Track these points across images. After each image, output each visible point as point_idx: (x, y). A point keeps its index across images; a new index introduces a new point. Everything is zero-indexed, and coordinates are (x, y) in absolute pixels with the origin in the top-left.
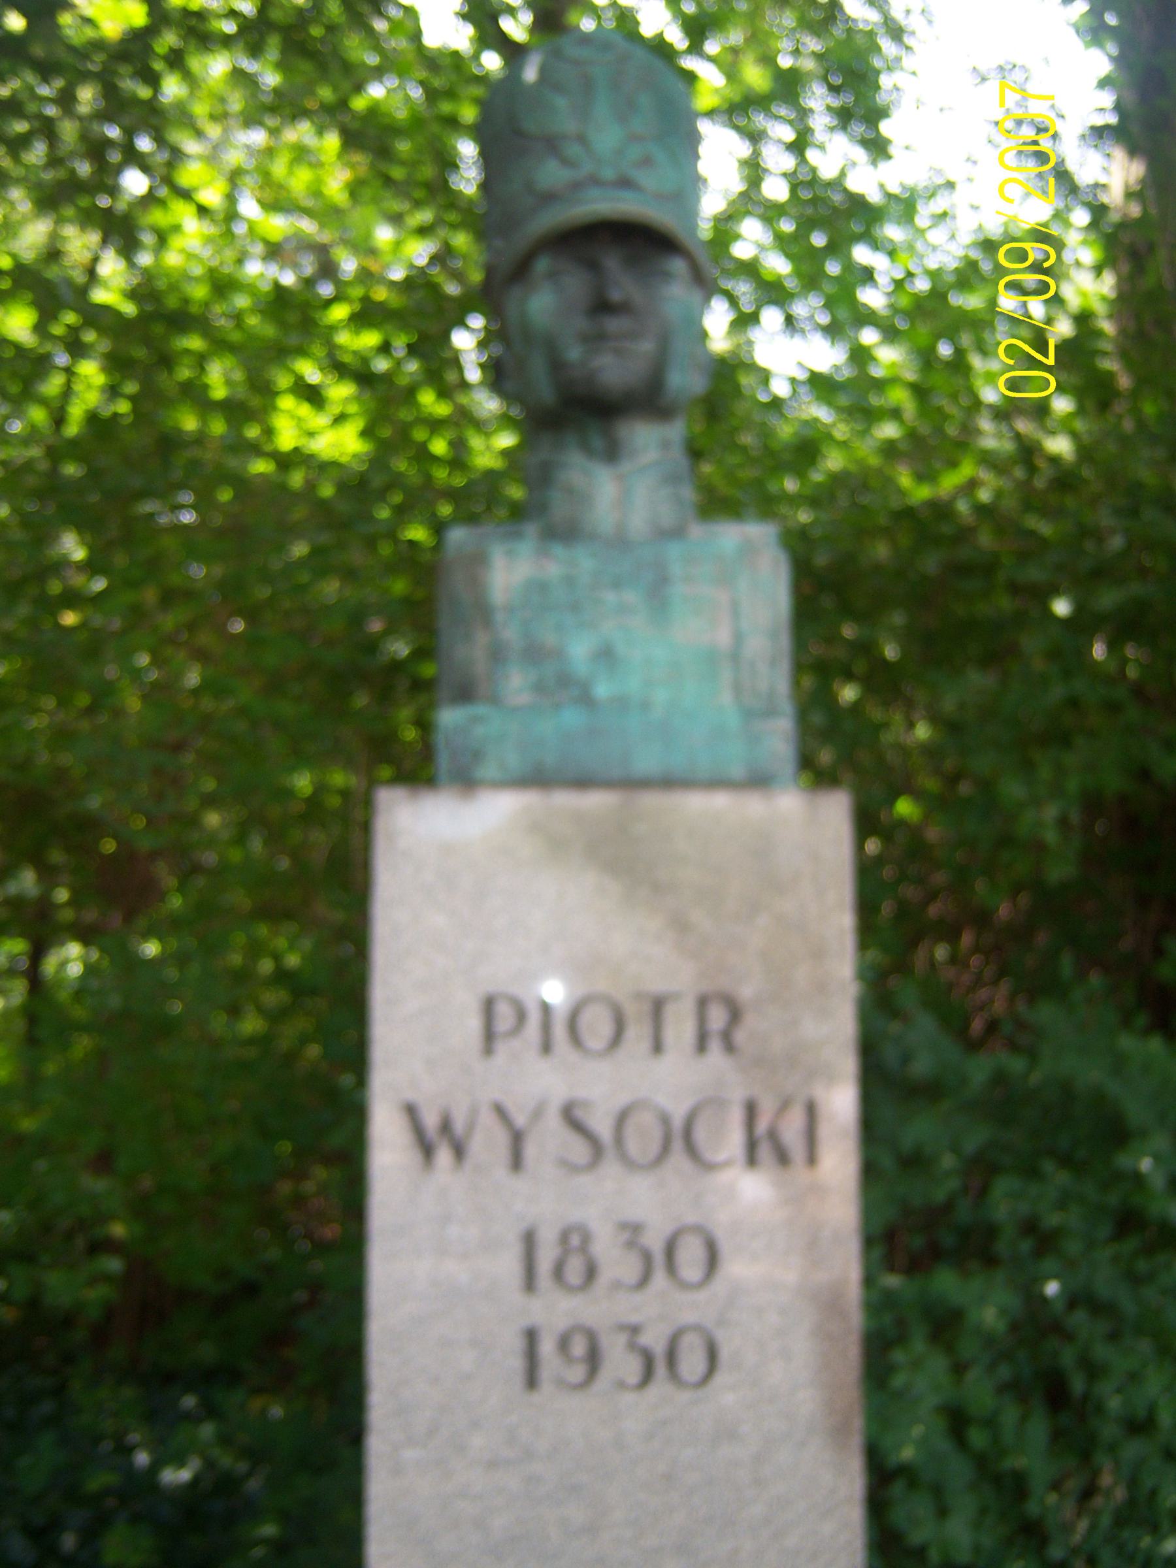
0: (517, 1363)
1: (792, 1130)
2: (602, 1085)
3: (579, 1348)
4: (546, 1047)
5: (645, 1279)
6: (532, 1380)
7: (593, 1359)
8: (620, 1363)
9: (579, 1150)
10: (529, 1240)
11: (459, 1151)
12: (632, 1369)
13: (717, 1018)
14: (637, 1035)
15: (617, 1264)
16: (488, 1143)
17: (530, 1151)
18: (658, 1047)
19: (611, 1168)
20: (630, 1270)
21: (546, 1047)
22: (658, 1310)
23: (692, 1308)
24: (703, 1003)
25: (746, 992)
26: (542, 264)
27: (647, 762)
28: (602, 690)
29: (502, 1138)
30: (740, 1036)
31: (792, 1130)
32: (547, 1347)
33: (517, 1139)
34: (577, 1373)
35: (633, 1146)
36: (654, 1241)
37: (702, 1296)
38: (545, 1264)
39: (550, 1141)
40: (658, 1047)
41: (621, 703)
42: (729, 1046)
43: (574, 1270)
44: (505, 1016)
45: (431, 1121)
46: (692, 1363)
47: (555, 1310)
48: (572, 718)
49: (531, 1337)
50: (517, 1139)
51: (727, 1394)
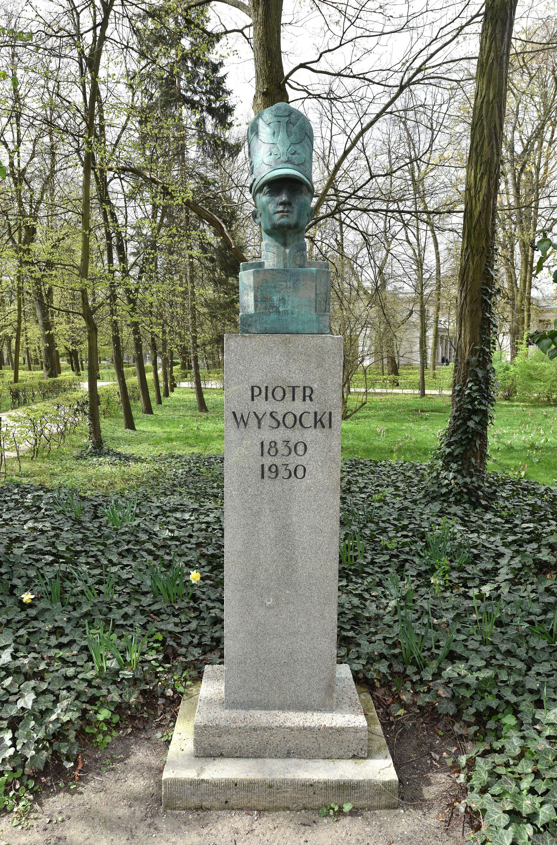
0: (260, 472)
1: (325, 421)
2: (280, 408)
3: (273, 469)
4: (266, 399)
5: (290, 453)
6: (263, 477)
7: (277, 472)
8: (283, 473)
9: (275, 424)
10: (262, 443)
11: (246, 425)
12: (286, 474)
14: (289, 396)
16: (253, 422)
17: (263, 423)
18: (294, 399)
19: (282, 428)
20: (286, 452)
21: (266, 399)
22: (293, 461)
24: (304, 388)
25: (315, 386)
26: (265, 188)
27: (292, 328)
28: (281, 309)
29: (256, 421)
30: (313, 397)
31: (325, 421)
32: (266, 469)
34: (273, 475)
35: (287, 422)
36: (291, 445)
37: (303, 458)
39: (267, 421)
40: (294, 399)
41: (286, 312)
42: (311, 399)
43: (273, 452)
44: (257, 391)
45: (239, 416)
46: (300, 473)
47: (268, 461)
48: (273, 316)
49: (263, 466)
51: (308, 480)
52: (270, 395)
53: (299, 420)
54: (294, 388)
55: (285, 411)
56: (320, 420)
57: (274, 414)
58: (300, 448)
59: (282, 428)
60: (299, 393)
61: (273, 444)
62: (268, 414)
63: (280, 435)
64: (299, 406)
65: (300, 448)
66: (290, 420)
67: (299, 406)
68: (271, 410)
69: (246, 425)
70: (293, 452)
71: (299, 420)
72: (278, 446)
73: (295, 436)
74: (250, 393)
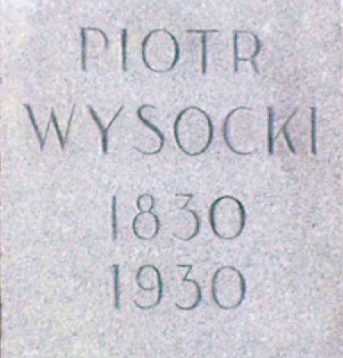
2: (163, 96)
3: (150, 279)
12: (187, 295)
13: (246, 47)
14: (190, 57)
15: (177, 222)
16: (84, 133)
17: (113, 140)
19: (171, 152)
23: (226, 253)
25: (266, 30)
32: (126, 278)
33: (104, 132)
37: (235, 244)
38: (125, 222)
45: (43, 119)
46: (229, 291)
49: (116, 270)
50: (104, 132)
52: (134, 53)
53: (218, 133)
54: (204, 36)
55: (180, 105)
56: (284, 129)
57: (145, 114)
58: (227, 215)
59: (171, 152)
60: (221, 53)
61: (146, 204)
62: (132, 116)
63: (171, 176)
64: (219, 90)
65: (227, 215)
66: (193, 132)
67: (219, 90)
68: (136, 100)
69: (62, 141)
70: (206, 228)
71: (218, 133)
72: (158, 210)
73: (204, 178)
74: (74, 47)
